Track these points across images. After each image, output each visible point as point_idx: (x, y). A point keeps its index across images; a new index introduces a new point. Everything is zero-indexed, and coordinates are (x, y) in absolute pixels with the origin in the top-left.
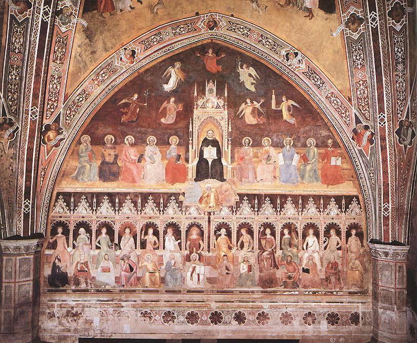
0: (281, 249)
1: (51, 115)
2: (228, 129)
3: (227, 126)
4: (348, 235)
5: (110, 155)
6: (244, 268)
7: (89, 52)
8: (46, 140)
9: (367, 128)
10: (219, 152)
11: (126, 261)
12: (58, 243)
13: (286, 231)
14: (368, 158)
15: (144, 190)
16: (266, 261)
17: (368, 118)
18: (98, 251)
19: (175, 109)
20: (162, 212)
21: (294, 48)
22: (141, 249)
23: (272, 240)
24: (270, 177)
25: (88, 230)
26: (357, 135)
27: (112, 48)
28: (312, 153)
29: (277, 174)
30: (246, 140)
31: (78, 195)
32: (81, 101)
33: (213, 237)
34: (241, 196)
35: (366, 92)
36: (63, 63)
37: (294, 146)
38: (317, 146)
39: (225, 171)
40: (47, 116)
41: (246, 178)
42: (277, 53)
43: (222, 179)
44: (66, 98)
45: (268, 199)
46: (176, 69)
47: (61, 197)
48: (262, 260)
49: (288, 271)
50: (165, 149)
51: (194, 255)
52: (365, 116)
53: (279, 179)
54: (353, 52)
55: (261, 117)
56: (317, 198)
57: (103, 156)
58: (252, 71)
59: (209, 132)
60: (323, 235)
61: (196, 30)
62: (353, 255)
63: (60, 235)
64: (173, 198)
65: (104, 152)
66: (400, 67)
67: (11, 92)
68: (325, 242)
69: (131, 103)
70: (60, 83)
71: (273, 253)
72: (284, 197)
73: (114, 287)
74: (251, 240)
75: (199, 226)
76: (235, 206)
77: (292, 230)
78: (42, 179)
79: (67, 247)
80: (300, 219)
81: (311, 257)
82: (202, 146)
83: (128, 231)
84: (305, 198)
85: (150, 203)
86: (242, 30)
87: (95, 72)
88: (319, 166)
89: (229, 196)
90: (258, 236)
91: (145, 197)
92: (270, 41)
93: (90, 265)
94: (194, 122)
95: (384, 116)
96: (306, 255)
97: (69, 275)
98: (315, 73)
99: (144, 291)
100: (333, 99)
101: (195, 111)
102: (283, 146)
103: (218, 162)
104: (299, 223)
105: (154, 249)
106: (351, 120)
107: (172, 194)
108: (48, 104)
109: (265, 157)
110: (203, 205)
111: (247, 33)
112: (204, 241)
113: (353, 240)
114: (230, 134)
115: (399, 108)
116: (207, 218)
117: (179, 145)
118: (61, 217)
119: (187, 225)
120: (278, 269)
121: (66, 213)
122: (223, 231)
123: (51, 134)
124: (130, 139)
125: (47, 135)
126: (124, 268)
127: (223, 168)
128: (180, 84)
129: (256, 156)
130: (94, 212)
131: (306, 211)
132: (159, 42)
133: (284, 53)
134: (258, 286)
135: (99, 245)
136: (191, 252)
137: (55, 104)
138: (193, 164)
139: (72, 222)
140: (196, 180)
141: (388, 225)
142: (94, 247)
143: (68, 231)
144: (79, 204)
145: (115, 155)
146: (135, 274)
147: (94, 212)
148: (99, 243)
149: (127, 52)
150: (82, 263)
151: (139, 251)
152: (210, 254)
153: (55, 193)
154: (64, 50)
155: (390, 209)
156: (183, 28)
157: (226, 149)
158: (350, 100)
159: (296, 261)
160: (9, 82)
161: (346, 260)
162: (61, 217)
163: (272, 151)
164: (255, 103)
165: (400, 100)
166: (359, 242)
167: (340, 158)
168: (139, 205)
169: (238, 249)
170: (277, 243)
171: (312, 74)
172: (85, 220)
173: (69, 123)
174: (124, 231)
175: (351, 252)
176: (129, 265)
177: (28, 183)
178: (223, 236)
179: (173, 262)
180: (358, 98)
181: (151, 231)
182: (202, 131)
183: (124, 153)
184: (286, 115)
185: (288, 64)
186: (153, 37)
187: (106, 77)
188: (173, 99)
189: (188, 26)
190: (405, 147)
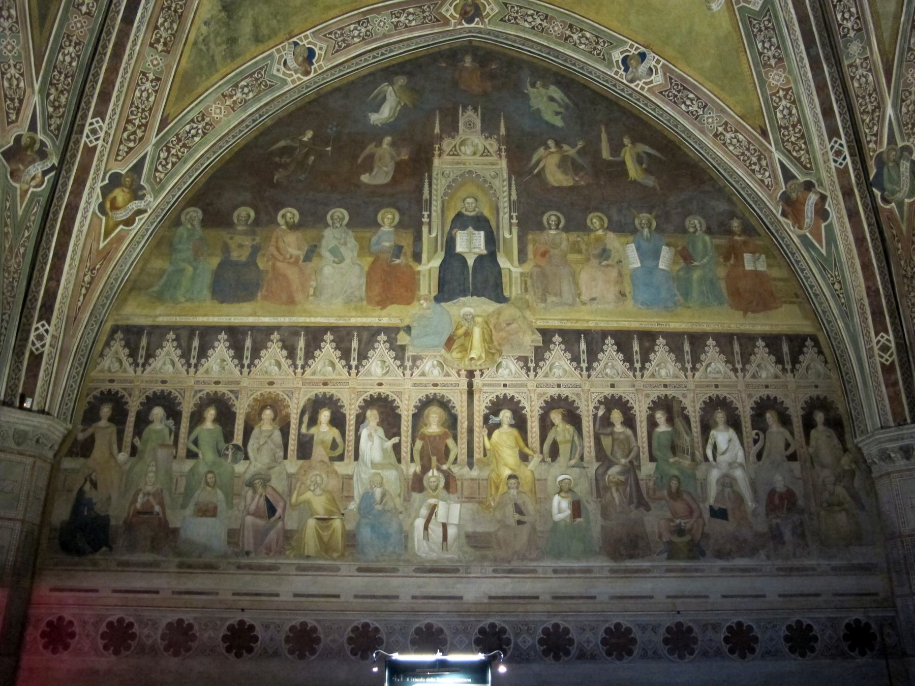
0: (652, 459)
1: (127, 153)
2: (510, 195)
3: (506, 188)
4: (809, 424)
5: (240, 246)
6: (560, 507)
7: (224, 38)
8: (108, 205)
9: (809, 186)
10: (491, 241)
11: (260, 490)
12: (98, 443)
13: (660, 416)
14: (824, 252)
15: (313, 320)
16: (617, 490)
17: (808, 166)
18: (189, 464)
19: (392, 158)
20: (354, 371)
21: (636, 45)
22: (299, 458)
23: (628, 438)
24: (611, 295)
25: (173, 413)
26: (792, 207)
27: (270, 38)
28: (700, 246)
29: (628, 289)
30: (550, 217)
31: (158, 332)
32: (193, 136)
33: (480, 431)
34: (546, 334)
35: (794, 111)
36: (168, 52)
37: (659, 229)
38: (709, 231)
39: (505, 280)
40: (118, 155)
41: (555, 295)
42: (604, 59)
43: (500, 298)
44: (164, 123)
45: (609, 341)
46: (396, 87)
47: (119, 335)
48: (607, 489)
49: (675, 514)
50: (368, 235)
51: (433, 476)
52: (801, 163)
53: (635, 299)
54: (755, 36)
55: (581, 174)
56: (725, 340)
57: (226, 249)
58: (555, 92)
59: (469, 200)
61: (438, 20)
62: (826, 473)
63: (103, 423)
64: (382, 337)
65: (229, 242)
66: (855, 48)
67: (57, 89)
68: (756, 442)
69: (296, 148)
70: (156, 92)
71: (632, 468)
72: (648, 338)
73: (225, 556)
74: (576, 438)
75: (444, 404)
76: (531, 356)
77: (675, 415)
78: (84, 291)
79: (115, 447)
80: (692, 387)
81: (727, 480)
82: (452, 228)
83: (268, 413)
84: (697, 340)
85: (328, 350)
86: (530, 19)
87: (229, 80)
88: (721, 272)
89: (517, 332)
90: (592, 429)
91: (315, 336)
92: (588, 35)
93: (167, 500)
94: (434, 181)
95: (841, 145)
96: (715, 474)
97: (113, 522)
98: (685, 88)
99: (300, 568)
100: (728, 136)
101: (436, 162)
102: (634, 231)
103: (488, 260)
104: (690, 396)
105: (332, 459)
106: (774, 175)
107: (378, 330)
108: (125, 129)
109: (597, 252)
110: (456, 355)
111: (541, 24)
112: (459, 441)
113: (821, 435)
114: (512, 206)
115: (867, 131)
116: (464, 382)
117: (400, 226)
118: (112, 381)
119: (415, 401)
120: (648, 509)
121: (125, 371)
122: (506, 415)
123: (120, 195)
124: (290, 214)
125: (111, 196)
126: (253, 507)
127: (500, 273)
128: (403, 113)
129: (575, 248)
130: (192, 370)
132: (364, 39)
133: (617, 56)
135: (193, 448)
136: (426, 468)
137: (140, 133)
138: (431, 265)
139: (137, 393)
140: (438, 299)
141: (896, 383)
142: (182, 452)
143: (125, 414)
144: (158, 351)
145: (253, 247)
146: (280, 524)
147: (192, 370)
148: (196, 442)
149: (298, 50)
150: (148, 494)
151: (292, 465)
152: (475, 473)
153: (108, 327)
154: (175, 26)
155: (893, 345)
156: (413, 14)
157: (509, 235)
158: (764, 133)
160: (55, 67)
162: (112, 381)
163: (613, 241)
164: (566, 147)
165: (868, 113)
166: (836, 441)
167: (763, 256)
168: (300, 353)
169: (543, 461)
170: (640, 444)
171: (679, 91)
172: (167, 388)
173: (161, 180)
174: (260, 414)
175: (823, 466)
176: (267, 500)
177: (53, 284)
178: (505, 427)
179: (378, 492)
180: (780, 127)
181: (325, 415)
182: (451, 198)
183: (273, 240)
184: (633, 171)
185: (629, 77)
186: (352, 27)
187: (251, 95)
188: (388, 140)
189: (424, 12)
190: (900, 205)
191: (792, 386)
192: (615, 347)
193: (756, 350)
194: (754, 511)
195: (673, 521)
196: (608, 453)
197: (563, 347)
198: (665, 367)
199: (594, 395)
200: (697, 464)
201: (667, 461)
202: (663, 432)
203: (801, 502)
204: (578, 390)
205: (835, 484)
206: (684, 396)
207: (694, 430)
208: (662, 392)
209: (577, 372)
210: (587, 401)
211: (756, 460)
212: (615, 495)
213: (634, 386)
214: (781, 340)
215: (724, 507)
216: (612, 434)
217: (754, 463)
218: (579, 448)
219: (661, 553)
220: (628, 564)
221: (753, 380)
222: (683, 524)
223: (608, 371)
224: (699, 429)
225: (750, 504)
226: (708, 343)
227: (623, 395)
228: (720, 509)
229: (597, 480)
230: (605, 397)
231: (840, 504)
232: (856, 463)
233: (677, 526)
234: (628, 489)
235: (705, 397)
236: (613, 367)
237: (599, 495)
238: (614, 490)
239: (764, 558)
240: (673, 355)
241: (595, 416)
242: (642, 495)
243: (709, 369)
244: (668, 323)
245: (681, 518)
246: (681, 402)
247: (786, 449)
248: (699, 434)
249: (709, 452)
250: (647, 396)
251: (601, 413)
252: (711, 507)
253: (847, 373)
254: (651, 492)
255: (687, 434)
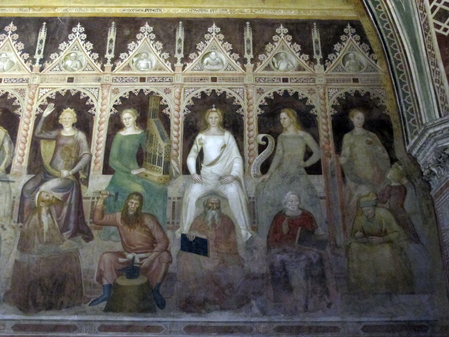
0: (107, 170)
16: (49, 212)
23: (78, 144)
45: (79, 28)
48: (35, 209)
60: (254, 126)
62: (364, 190)
68: (261, 148)
74: (6, 144)
80: (179, 79)
81: (214, 200)
90: (30, 132)
104: (175, 91)
131: (196, 60)
134: (4, 301)
159: (159, 214)
161: (342, 208)
166: (380, 148)
175: (359, 182)
191: (321, 80)
192: (84, 36)
193: (275, 38)
194: (250, 242)
195: (124, 257)
196: (47, 161)
197: (16, 36)
198: (147, 58)
199: (43, 91)
200: (171, 178)
201: (128, 173)
202: (130, 137)
203: (321, 231)
204: (20, 86)
205: (376, 206)
206: (167, 91)
207: (174, 133)
208: (137, 86)
209: (27, 65)
210: (32, 99)
211: (259, 174)
212: (45, 219)
213: (99, 80)
214: (311, 27)
215: (204, 237)
216: (57, 138)
217: (256, 176)
218: (7, 157)
219: (96, 302)
220: (44, 318)
221: (266, 72)
222: (137, 260)
223: (69, 63)
224: (181, 132)
225: (243, 232)
226: (210, 30)
227: (83, 91)
228: (197, 238)
229: (22, 198)
230: (58, 94)
231: (382, 233)
232: (408, 177)
233: (128, 262)
234: (65, 210)
235: (197, 93)
236: (76, 58)
237: (21, 219)
238: (44, 211)
239: (256, 310)
240: (160, 45)
241: (39, 116)
242: (83, 217)
243: (206, 60)
244: (159, 8)
245: (137, 251)
246: (161, 98)
247: (305, 159)
248: (180, 138)
249: (191, 162)
250: (115, 91)
251: (47, 113)
252: (184, 237)
253: (397, 62)
254: (97, 215)
255: (163, 138)
